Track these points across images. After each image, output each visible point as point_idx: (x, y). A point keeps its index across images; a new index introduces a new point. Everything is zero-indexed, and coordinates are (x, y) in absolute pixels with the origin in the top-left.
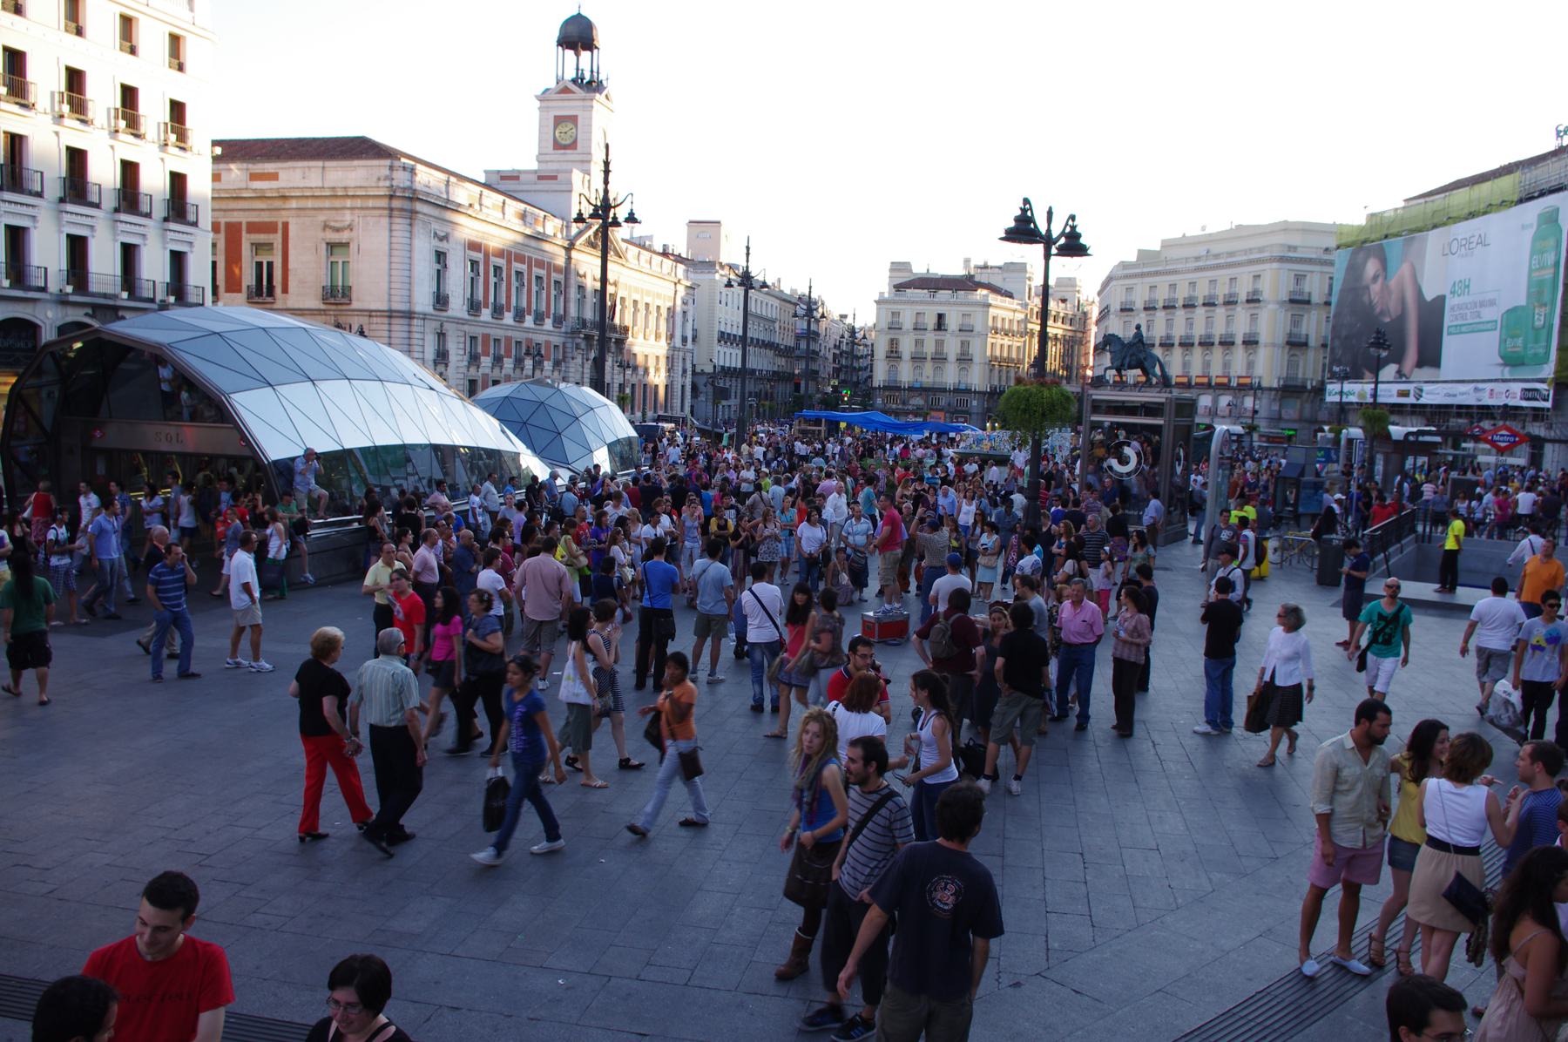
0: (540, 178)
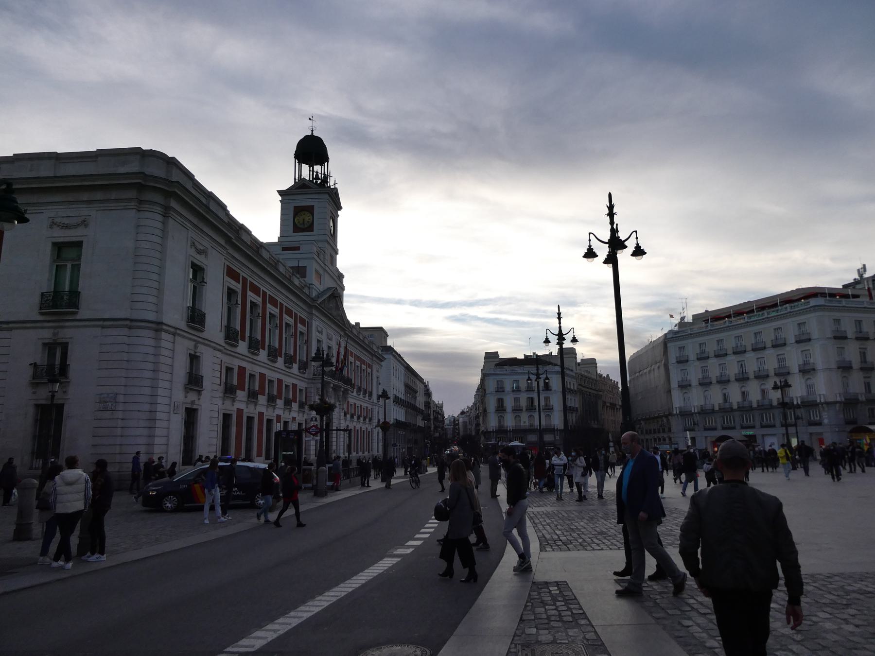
0: (284, 249)
